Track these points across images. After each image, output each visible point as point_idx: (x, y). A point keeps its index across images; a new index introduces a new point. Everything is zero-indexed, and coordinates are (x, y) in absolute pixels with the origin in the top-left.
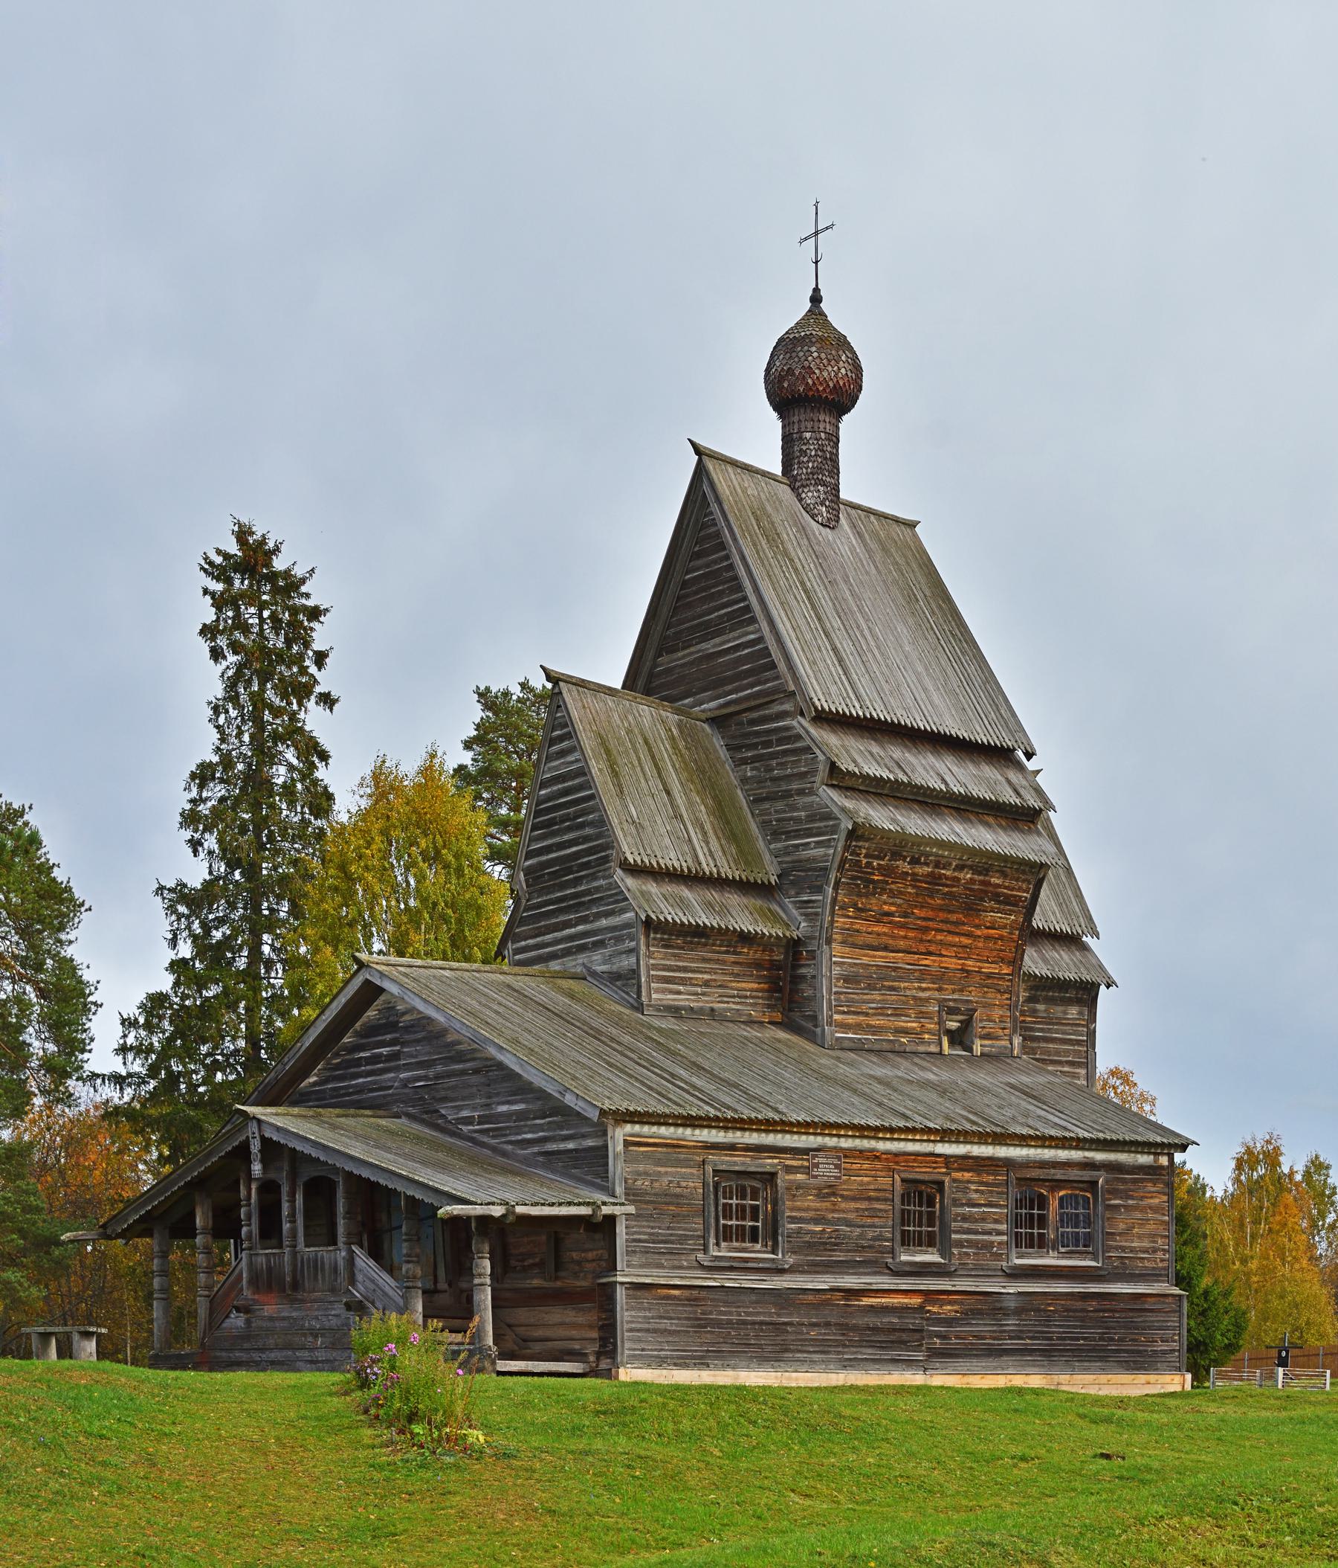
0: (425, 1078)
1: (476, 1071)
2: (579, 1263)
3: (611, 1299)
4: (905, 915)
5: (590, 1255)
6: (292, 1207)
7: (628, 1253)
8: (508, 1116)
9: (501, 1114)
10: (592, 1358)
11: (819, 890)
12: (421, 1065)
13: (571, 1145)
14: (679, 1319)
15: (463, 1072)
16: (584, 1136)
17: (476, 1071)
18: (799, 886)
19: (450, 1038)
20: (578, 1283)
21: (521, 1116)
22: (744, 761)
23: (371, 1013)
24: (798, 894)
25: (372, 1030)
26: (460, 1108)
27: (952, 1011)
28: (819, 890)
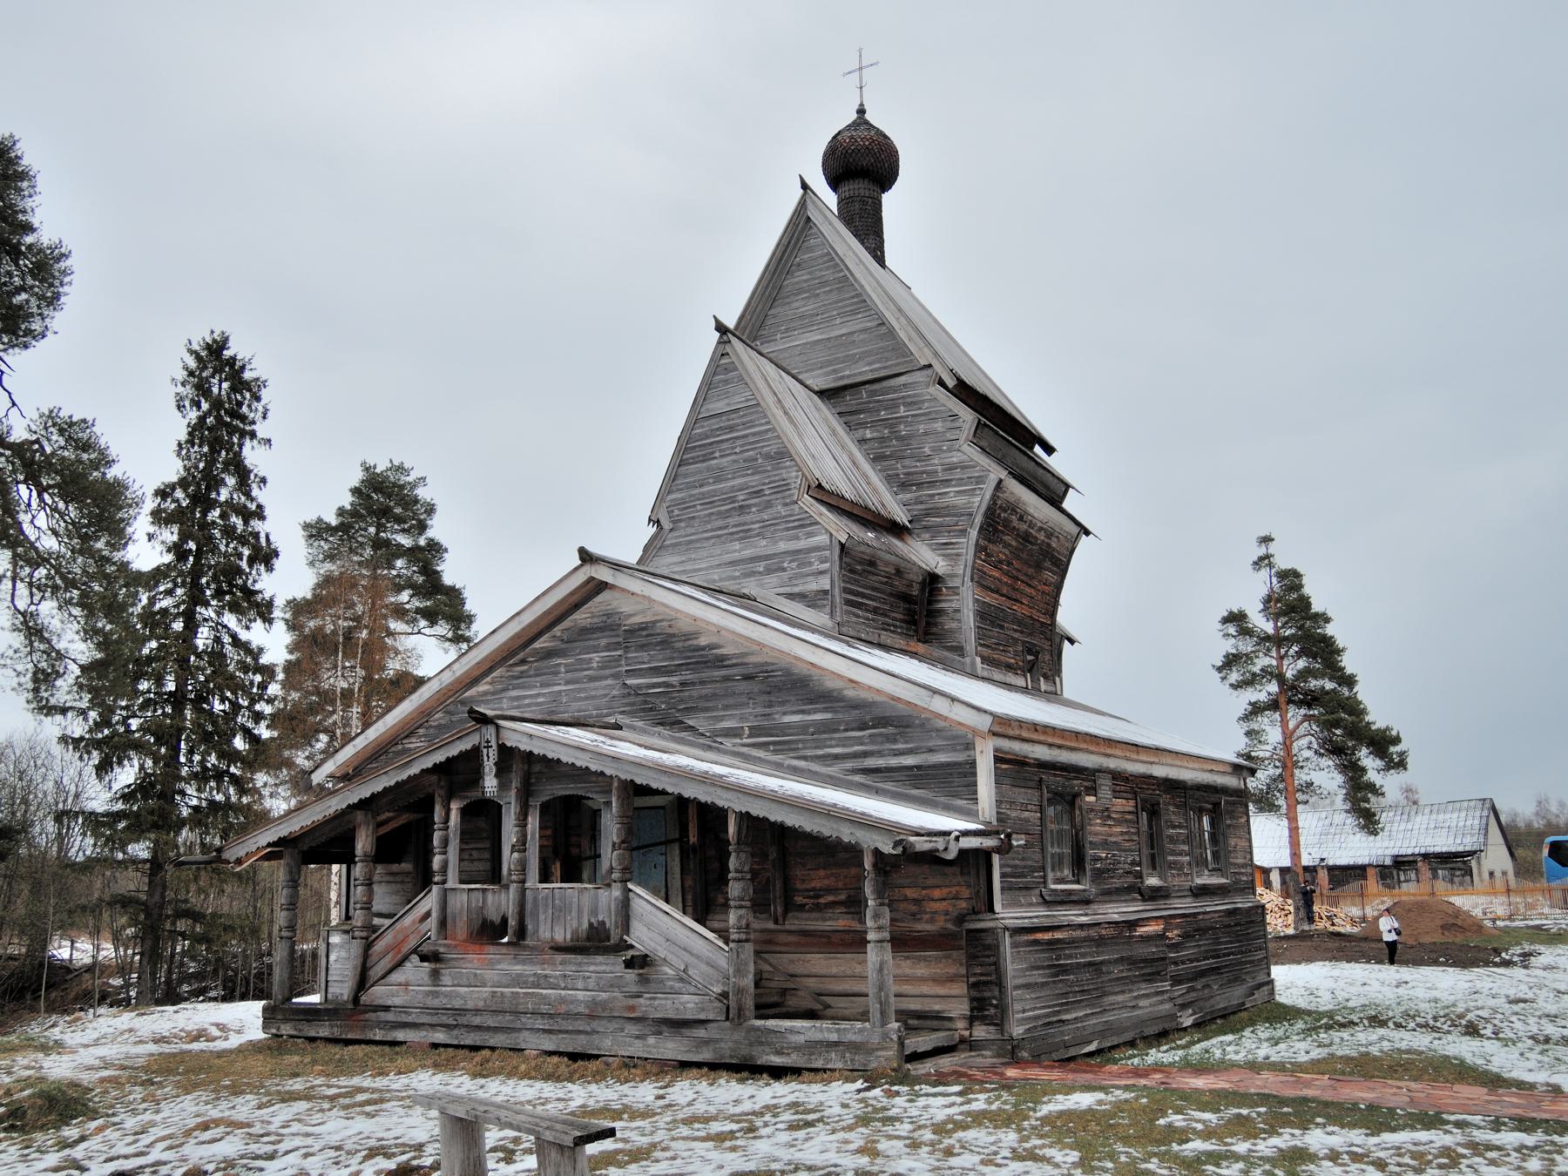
0: (666, 685)
1: (748, 677)
2: (917, 901)
3: (995, 949)
4: (1009, 564)
5: (937, 893)
6: (520, 834)
7: (1003, 889)
8: (803, 728)
9: (789, 725)
10: (960, 1024)
11: (963, 532)
12: (656, 671)
13: (909, 761)
14: (1043, 968)
15: (727, 679)
16: (931, 750)
17: (748, 677)
18: (934, 530)
19: (703, 641)
20: (919, 927)
21: (828, 728)
22: (863, 425)
23: (581, 617)
24: (933, 537)
25: (585, 632)
26: (722, 718)
27: (1030, 652)
28: (963, 532)
